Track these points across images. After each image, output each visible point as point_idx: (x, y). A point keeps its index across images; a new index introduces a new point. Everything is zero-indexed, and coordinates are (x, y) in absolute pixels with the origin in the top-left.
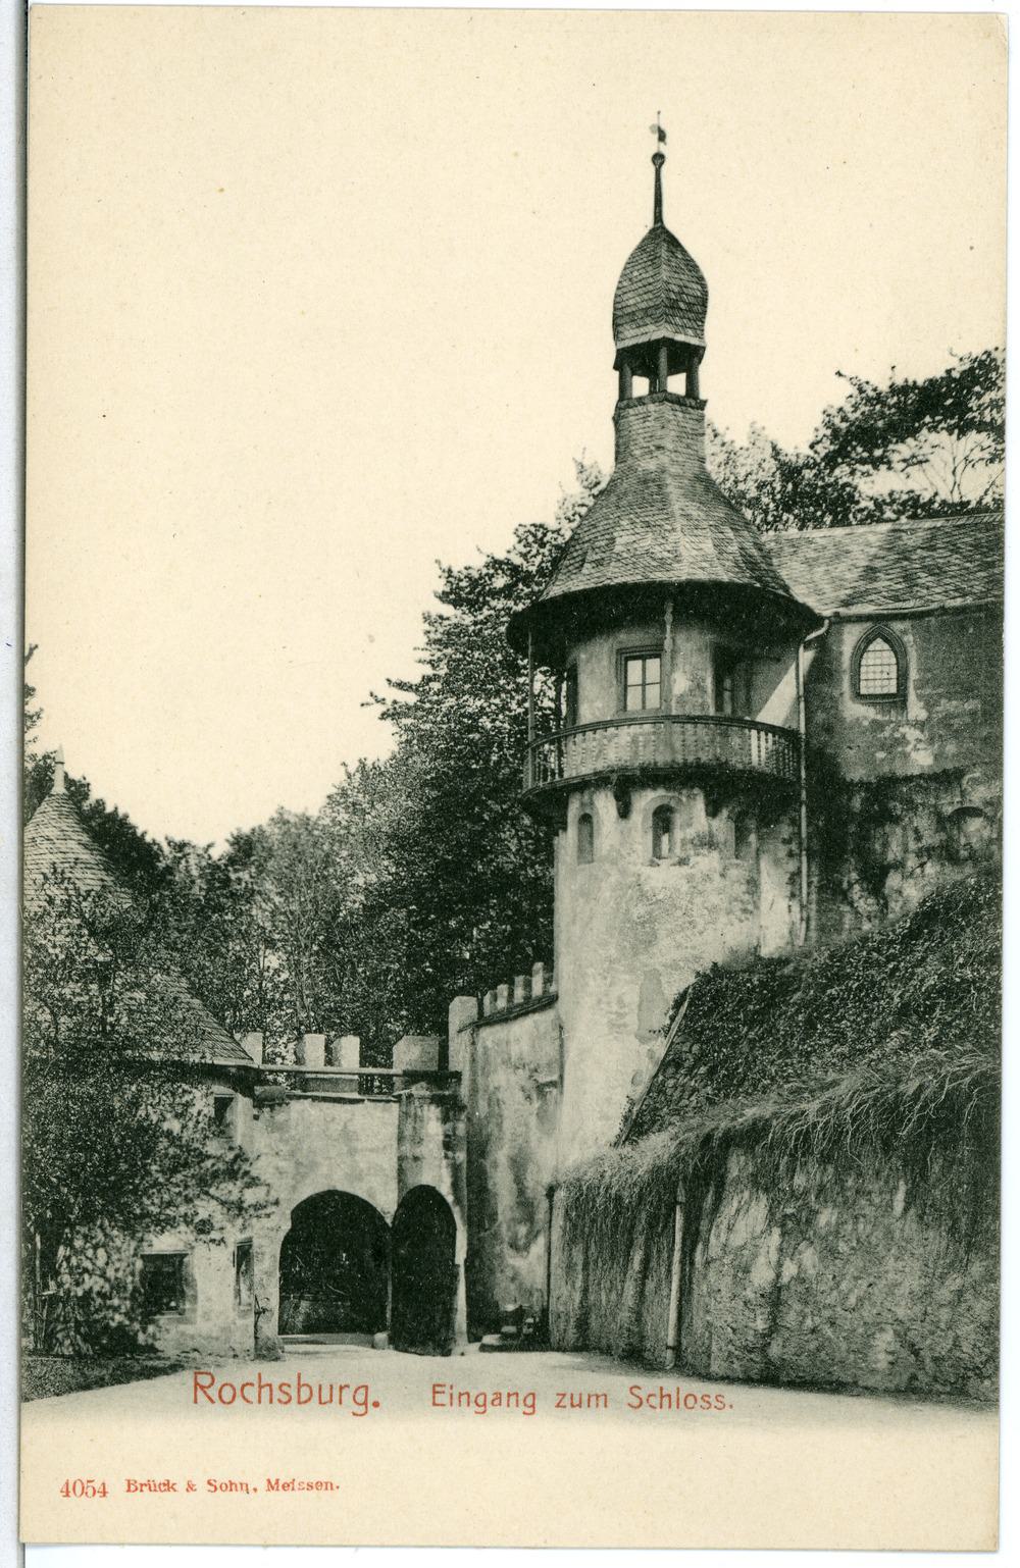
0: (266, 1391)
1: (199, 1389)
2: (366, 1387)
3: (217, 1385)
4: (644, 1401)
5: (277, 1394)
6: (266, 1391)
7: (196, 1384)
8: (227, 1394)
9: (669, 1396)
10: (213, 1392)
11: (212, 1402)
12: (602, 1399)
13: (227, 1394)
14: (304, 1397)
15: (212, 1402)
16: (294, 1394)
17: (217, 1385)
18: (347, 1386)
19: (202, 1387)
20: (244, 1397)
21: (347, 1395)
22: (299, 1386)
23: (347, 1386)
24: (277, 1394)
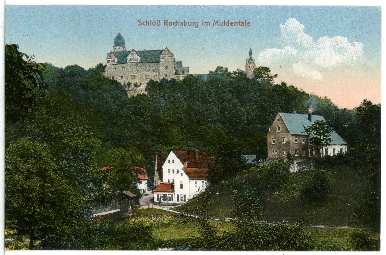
0: (178, 23)
1: (165, 24)
2: (198, 22)
3: (169, 22)
4: (173, 24)
5: (180, 24)
6: (178, 23)
7: (165, 22)
8: (171, 24)
9: (149, 22)
11: (167, 25)
12: (208, 23)
13: (171, 24)
15: (167, 25)
16: (183, 23)
17: (169, 22)
18: (194, 22)
19: (166, 23)
20: (174, 24)
21: (194, 24)
22: (185, 22)
23: (194, 22)
24: (180, 24)
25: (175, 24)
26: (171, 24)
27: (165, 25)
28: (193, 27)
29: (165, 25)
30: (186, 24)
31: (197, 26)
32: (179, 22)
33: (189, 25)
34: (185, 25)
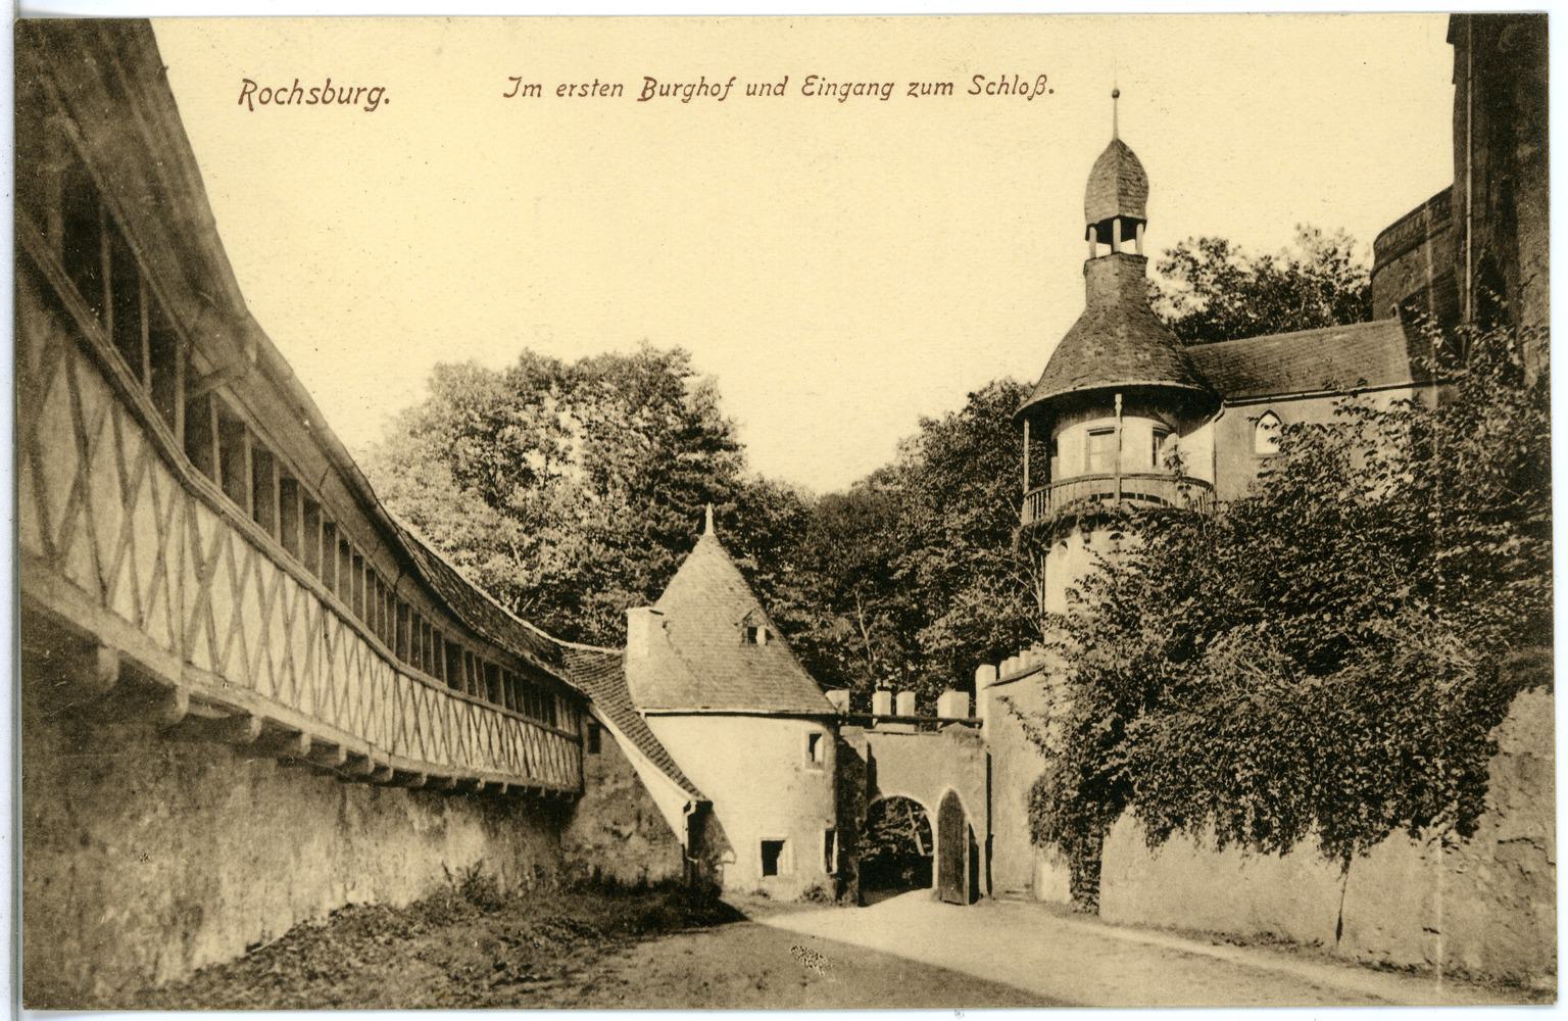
3: (259, 91)
5: (307, 96)
6: (298, 93)
7: (244, 93)
10: (255, 97)
14: (327, 98)
17: (259, 91)
21: (364, 95)
25: (282, 96)
26: (270, 96)
27: (241, 102)
28: (355, 110)
29: (241, 102)
30: (329, 95)
31: (371, 106)
32: (301, 90)
33: (340, 101)
34: (324, 102)
